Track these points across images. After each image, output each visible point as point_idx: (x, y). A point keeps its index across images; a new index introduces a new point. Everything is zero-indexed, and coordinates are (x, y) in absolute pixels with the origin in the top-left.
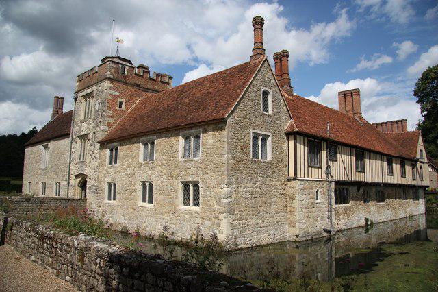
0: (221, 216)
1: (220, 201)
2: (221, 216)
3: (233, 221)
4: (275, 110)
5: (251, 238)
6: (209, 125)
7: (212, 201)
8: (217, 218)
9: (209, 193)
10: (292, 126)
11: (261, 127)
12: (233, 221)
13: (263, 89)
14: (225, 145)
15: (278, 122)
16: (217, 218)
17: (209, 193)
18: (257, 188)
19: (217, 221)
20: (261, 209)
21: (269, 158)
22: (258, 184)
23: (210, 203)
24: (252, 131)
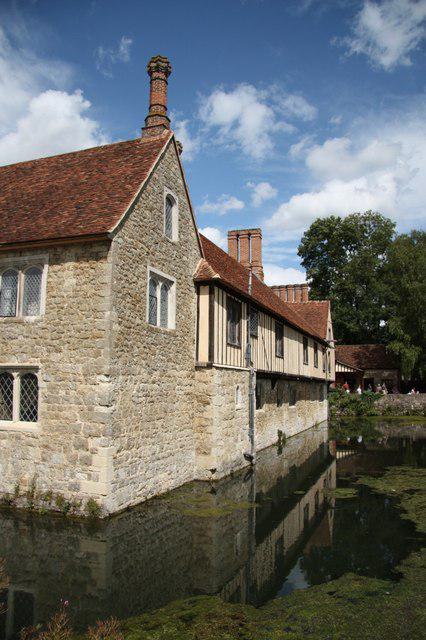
0: (92, 443)
1: (91, 409)
2: (92, 443)
3: (118, 451)
4: (182, 236)
5: (144, 483)
6: (65, 247)
7: (72, 411)
8: (83, 446)
9: (62, 393)
10: (205, 269)
11: (162, 263)
12: (118, 451)
13: (167, 192)
14: (107, 292)
15: (185, 258)
16: (83, 446)
17: (62, 393)
18: (154, 382)
19: (82, 453)
20: (159, 423)
21: (171, 325)
22: (156, 374)
23: (66, 413)
24: (150, 268)
